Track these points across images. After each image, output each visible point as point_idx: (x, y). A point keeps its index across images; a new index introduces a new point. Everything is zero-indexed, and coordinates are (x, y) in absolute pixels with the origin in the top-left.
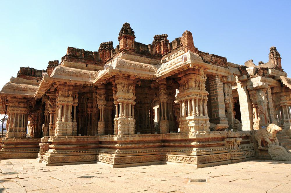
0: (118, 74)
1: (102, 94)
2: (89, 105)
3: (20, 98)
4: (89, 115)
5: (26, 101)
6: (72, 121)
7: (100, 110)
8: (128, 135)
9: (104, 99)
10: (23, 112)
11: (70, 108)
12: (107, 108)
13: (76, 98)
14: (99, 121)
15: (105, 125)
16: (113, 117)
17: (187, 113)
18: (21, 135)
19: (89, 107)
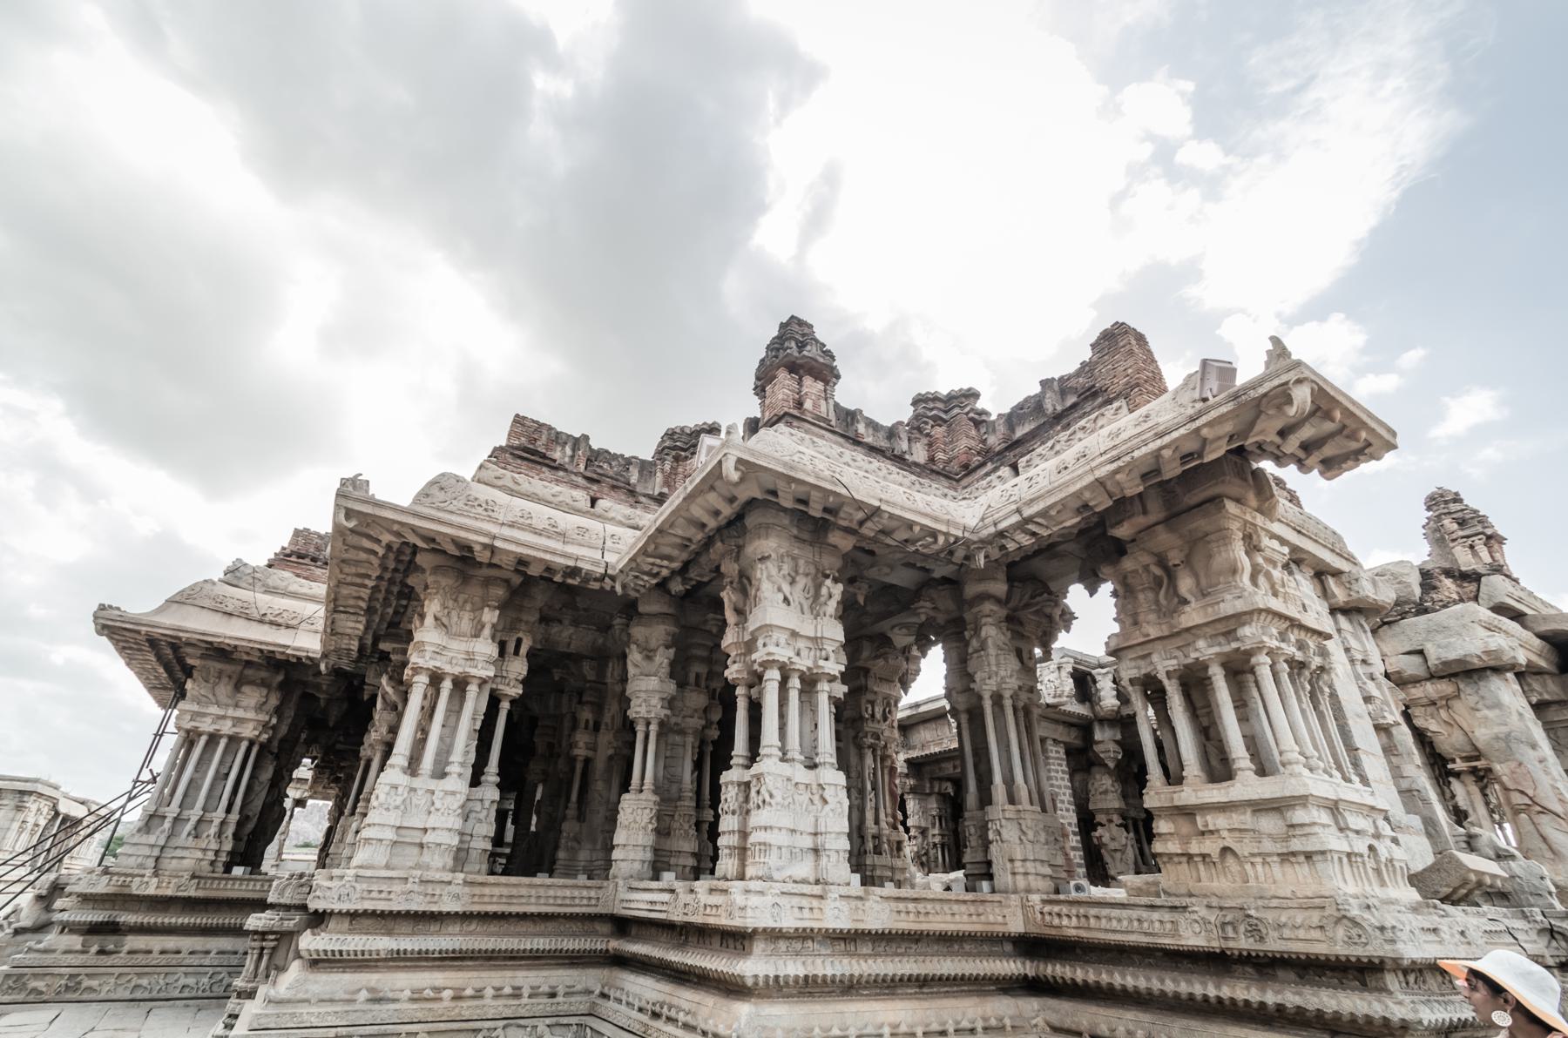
0: (774, 493)
1: (653, 644)
2: (586, 715)
3: (248, 664)
4: (579, 767)
5: (280, 678)
6: (475, 782)
7: (640, 729)
8: (817, 890)
9: (665, 670)
10: (248, 731)
11: (475, 703)
12: (673, 720)
13: (517, 653)
14: (625, 787)
15: (659, 817)
16: (722, 760)
17: (1172, 766)
18: (199, 855)
19: (582, 725)
